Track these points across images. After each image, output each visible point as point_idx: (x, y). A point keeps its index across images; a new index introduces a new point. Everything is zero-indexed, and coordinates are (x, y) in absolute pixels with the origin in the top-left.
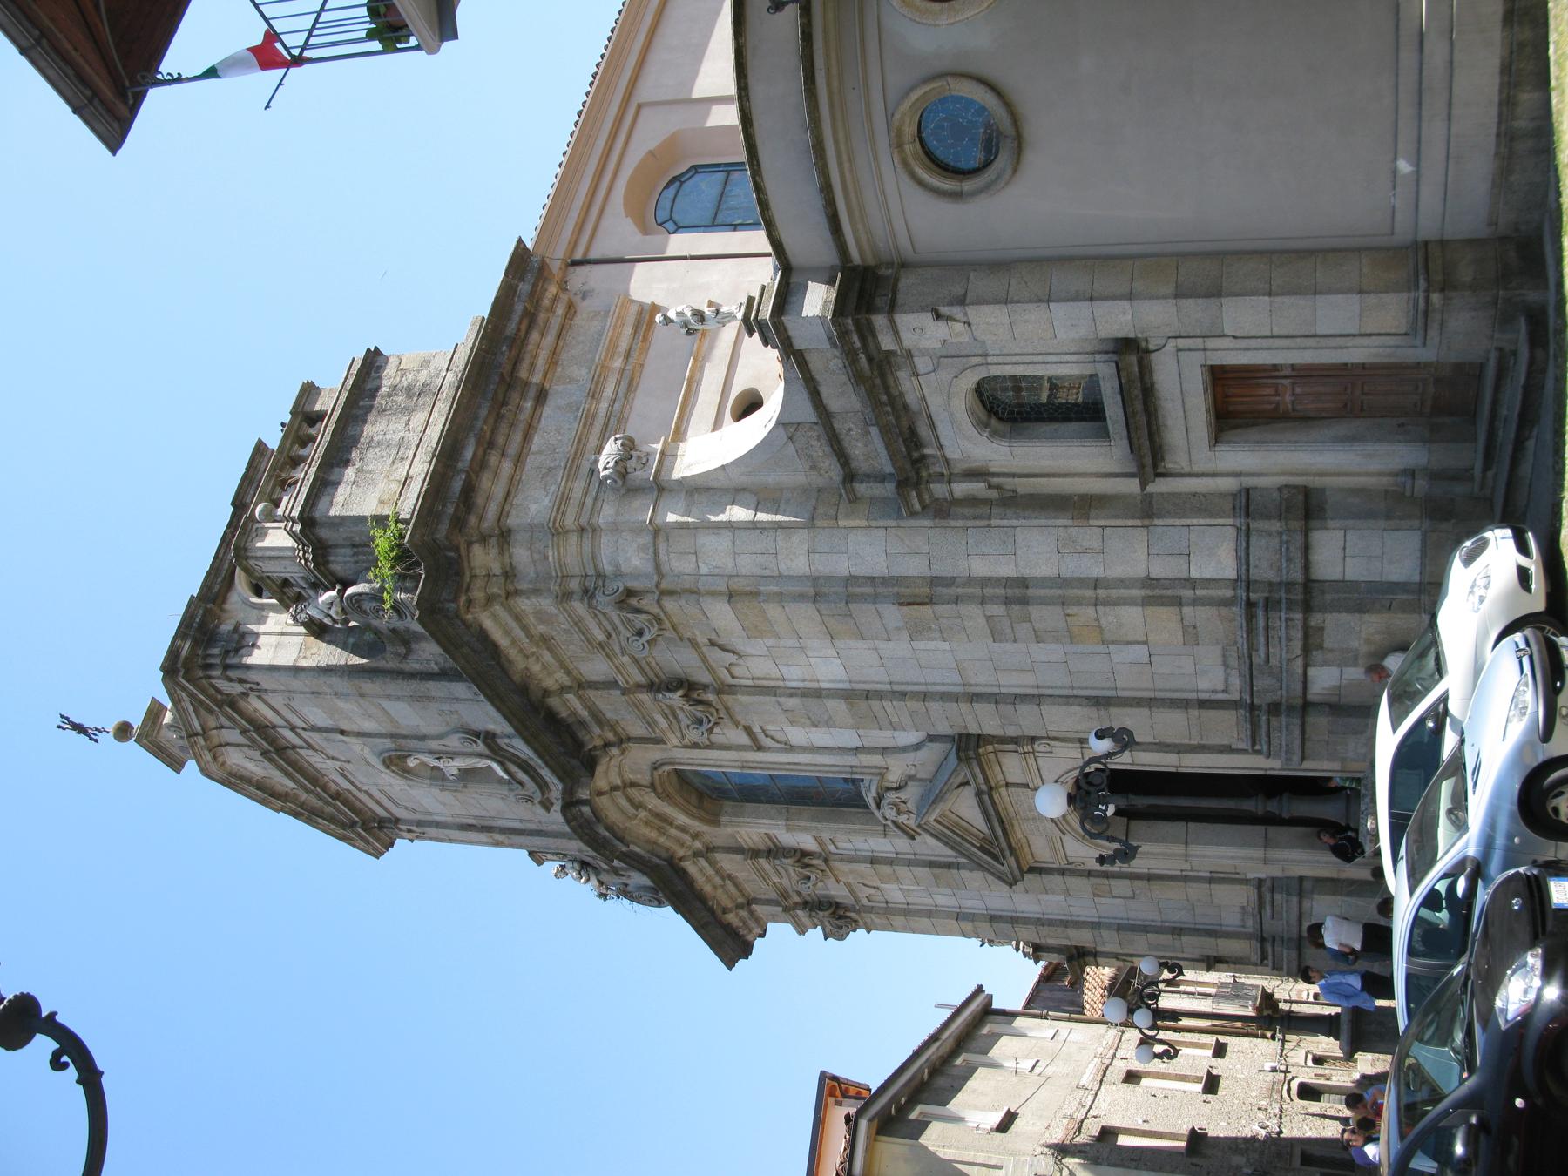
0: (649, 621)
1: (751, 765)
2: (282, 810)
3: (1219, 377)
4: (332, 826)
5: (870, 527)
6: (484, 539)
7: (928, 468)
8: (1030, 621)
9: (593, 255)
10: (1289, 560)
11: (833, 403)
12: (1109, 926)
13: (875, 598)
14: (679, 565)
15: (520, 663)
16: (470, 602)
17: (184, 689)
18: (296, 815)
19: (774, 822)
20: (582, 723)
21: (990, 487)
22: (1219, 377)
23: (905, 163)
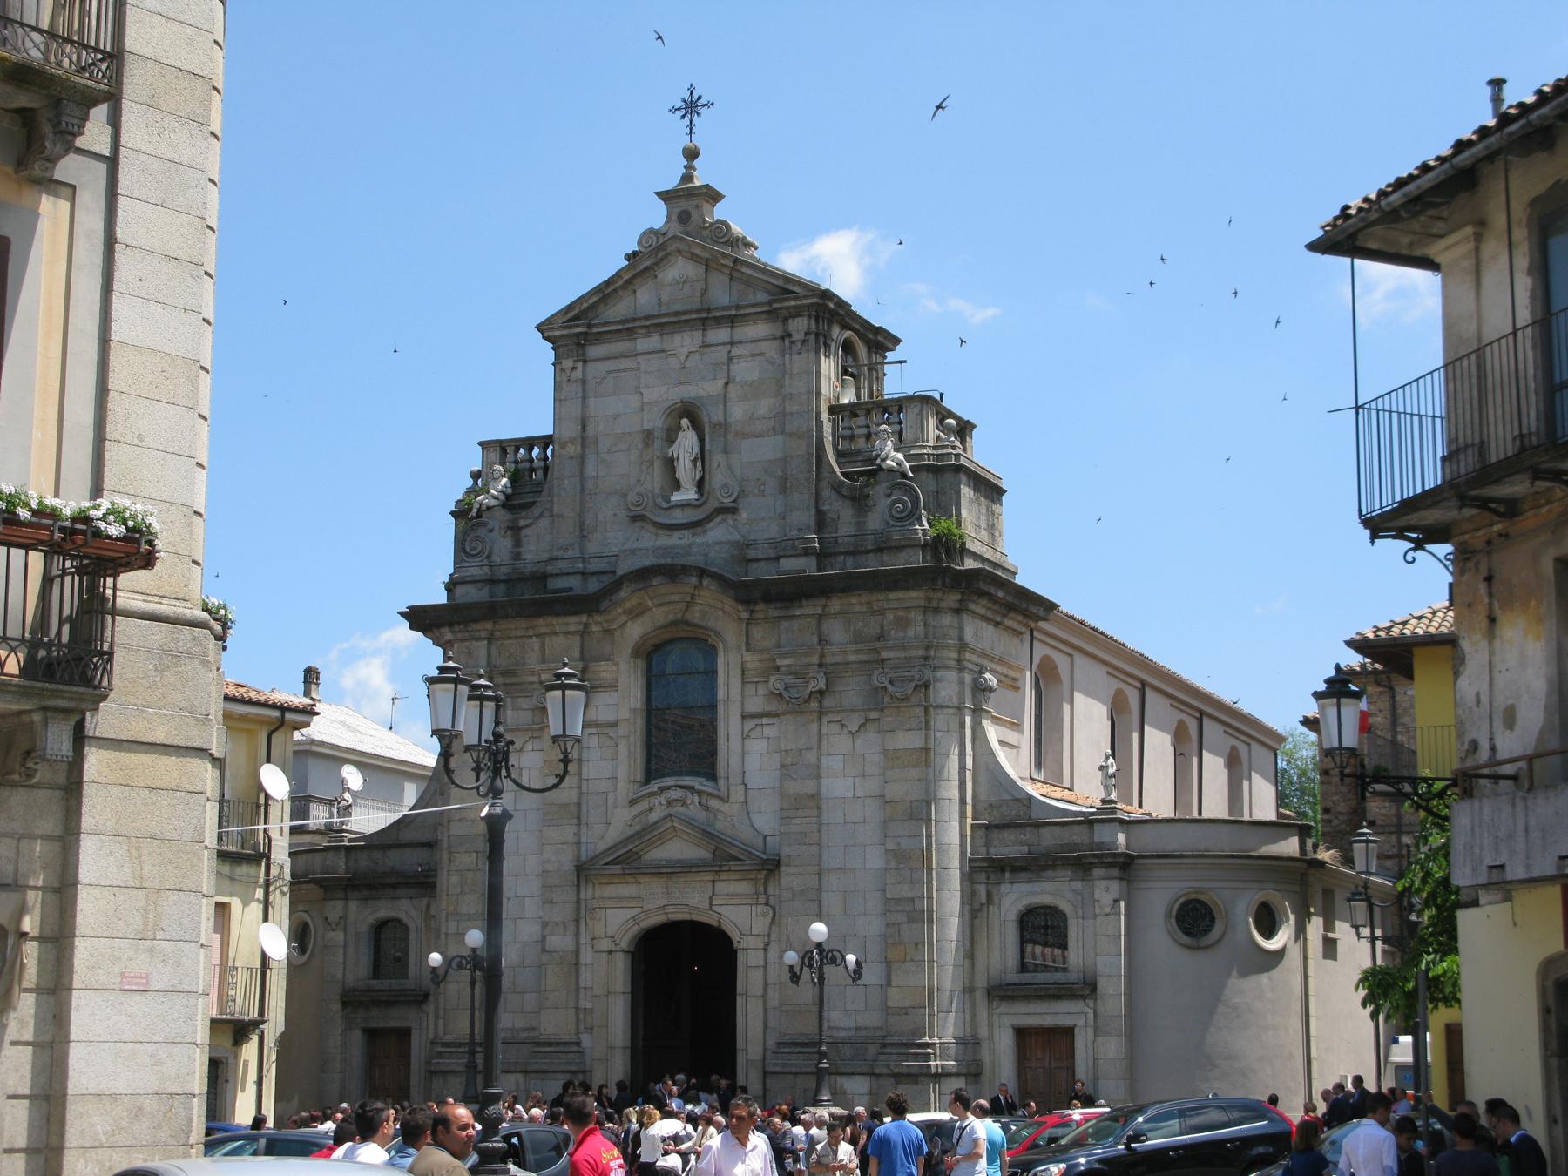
3: (1068, 1032)
6: (961, 601)
9: (1035, 642)
11: (1045, 831)
14: (940, 720)
15: (866, 597)
18: (608, 283)
21: (982, 905)
22: (1068, 1032)
23: (1189, 893)
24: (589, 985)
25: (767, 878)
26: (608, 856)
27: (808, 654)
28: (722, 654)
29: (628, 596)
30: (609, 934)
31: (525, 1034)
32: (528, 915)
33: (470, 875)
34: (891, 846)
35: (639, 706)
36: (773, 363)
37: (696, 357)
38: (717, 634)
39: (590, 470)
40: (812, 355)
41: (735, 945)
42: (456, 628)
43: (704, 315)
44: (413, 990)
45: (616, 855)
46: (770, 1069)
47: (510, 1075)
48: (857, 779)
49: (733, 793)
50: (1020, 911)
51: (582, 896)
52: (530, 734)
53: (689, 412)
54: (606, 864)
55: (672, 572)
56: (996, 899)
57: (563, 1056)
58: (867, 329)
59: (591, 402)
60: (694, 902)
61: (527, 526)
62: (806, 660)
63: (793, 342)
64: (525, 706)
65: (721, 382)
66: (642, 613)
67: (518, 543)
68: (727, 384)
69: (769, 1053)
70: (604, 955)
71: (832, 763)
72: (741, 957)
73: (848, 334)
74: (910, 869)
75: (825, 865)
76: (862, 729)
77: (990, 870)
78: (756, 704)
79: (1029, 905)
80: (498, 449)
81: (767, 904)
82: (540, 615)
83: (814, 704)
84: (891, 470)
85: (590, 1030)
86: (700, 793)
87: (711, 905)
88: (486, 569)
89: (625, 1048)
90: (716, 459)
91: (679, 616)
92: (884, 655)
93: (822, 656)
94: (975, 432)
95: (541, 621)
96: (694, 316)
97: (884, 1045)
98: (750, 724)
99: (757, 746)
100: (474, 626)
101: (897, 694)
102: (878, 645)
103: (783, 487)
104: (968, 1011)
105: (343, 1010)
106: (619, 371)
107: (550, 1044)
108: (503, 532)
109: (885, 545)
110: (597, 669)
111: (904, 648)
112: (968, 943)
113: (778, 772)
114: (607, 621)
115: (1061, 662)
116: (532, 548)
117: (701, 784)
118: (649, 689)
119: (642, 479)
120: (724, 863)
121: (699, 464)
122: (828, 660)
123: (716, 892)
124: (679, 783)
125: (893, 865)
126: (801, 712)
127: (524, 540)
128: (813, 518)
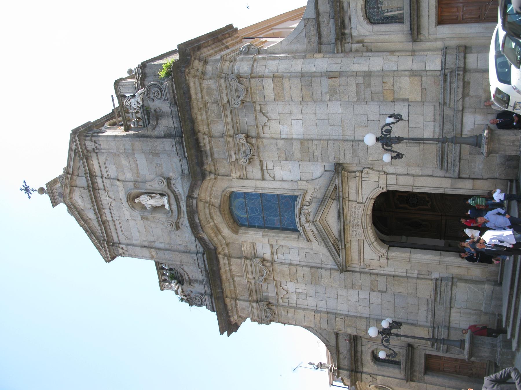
0: (244, 88)
1: (258, 188)
2: (82, 226)
4: (96, 241)
5: (324, 57)
6: (200, 60)
7: (345, 40)
8: (370, 87)
10: (459, 60)
12: (373, 319)
13: (321, 76)
14: (259, 69)
15: (195, 110)
16: (189, 73)
18: (86, 231)
19: (258, 233)
20: (206, 153)
24: (405, 271)
25: (348, 171)
26: (336, 257)
27: (228, 143)
28: (232, 189)
29: (208, 234)
30: (378, 258)
31: (430, 305)
32: (367, 297)
33: (347, 323)
34: (326, 98)
35: (261, 233)
36: (107, 158)
37: (110, 193)
38: (223, 191)
39: (162, 246)
40: (100, 139)
41: (384, 191)
42: (230, 314)
43: (91, 189)
44: (406, 351)
45: (335, 252)
46: (457, 176)
47: (451, 316)
48: (293, 118)
49: (302, 188)
50: (367, 22)
51: (358, 270)
52: (279, 286)
53: (132, 198)
54: (340, 256)
55: (192, 213)
56: (361, 38)
57: (443, 289)
58: (110, 116)
59: (135, 242)
60: (361, 213)
61: (188, 276)
62: (232, 145)
64: (266, 287)
65: (118, 182)
66: (217, 227)
67: (196, 281)
68: (118, 180)
69: (447, 175)
70: (389, 262)
71: (284, 131)
72: (391, 188)
73: (107, 125)
74: (340, 86)
75: (340, 138)
76: (266, 114)
77: (344, 41)
79: (364, 17)
80: (162, 282)
81: (362, 172)
82: (220, 278)
83: (254, 141)
84: (143, 100)
85: (429, 273)
86: (302, 206)
87: (362, 203)
88: (206, 297)
89: (441, 255)
90: (148, 186)
91: (217, 210)
92: (225, 101)
93: (230, 136)
95: (224, 277)
98: (267, 176)
99: (278, 173)
100: (229, 307)
101: (244, 93)
102: (220, 104)
103: (155, 154)
104: (426, 53)
105: (415, 381)
106: (121, 229)
107: (436, 294)
108: (192, 287)
109: (173, 102)
110: (246, 252)
111: (220, 90)
112: (385, 54)
113: (290, 162)
114: (222, 245)
116: (197, 275)
117: (298, 205)
119: (161, 222)
120: (338, 195)
121: (153, 195)
122: (231, 132)
123: (356, 200)
124: (298, 216)
125: (337, 96)
126: (258, 148)
127: (194, 278)
128: (167, 140)
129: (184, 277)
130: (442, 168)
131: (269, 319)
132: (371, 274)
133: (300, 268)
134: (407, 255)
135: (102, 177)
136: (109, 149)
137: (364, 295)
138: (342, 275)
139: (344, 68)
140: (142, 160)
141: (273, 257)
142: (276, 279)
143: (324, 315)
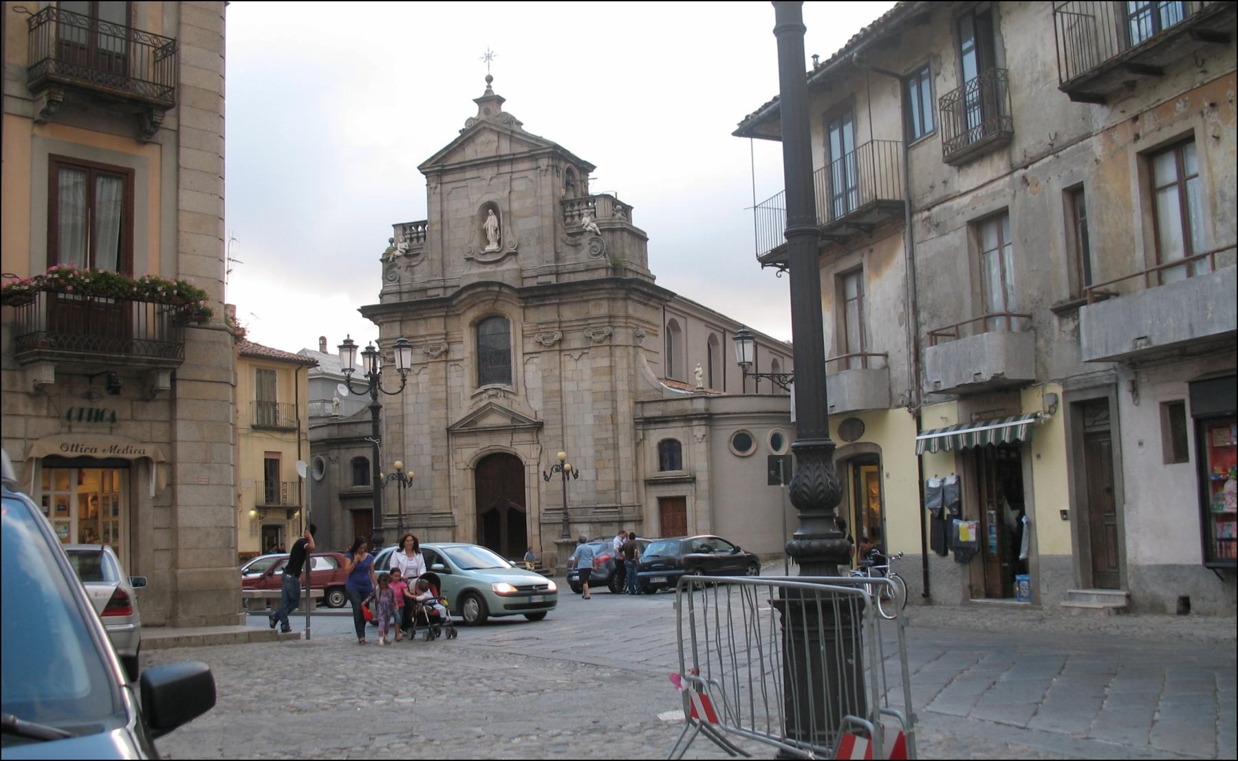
3: (683, 499)
6: (626, 294)
9: (666, 313)
13: (613, 409)
14: (618, 352)
17: (546, 148)
22: (683, 499)
35: (473, 350)
36: (532, 181)
37: (494, 181)
39: (446, 237)
42: (385, 316)
51: (450, 443)
53: (491, 207)
59: (445, 203)
63: (541, 171)
68: (510, 192)
69: (541, 515)
72: (526, 469)
73: (569, 165)
74: (606, 424)
75: (565, 424)
78: (530, 348)
83: (557, 347)
84: (590, 231)
85: (456, 507)
86: (504, 391)
90: (507, 228)
94: (633, 211)
96: (493, 159)
97: (596, 508)
98: (527, 357)
99: (531, 368)
103: (540, 240)
115: (681, 322)
118: (478, 341)
125: (597, 422)
129: (415, 259)
130: (546, 510)
131: (387, 357)
132: (448, 455)
133: (444, 388)
134: (470, 486)
135: (512, 172)
136: (541, 187)
137: (427, 449)
138: (443, 430)
139: (620, 426)
140: (530, 224)
141: (450, 361)
142: (430, 364)
143: (400, 412)
